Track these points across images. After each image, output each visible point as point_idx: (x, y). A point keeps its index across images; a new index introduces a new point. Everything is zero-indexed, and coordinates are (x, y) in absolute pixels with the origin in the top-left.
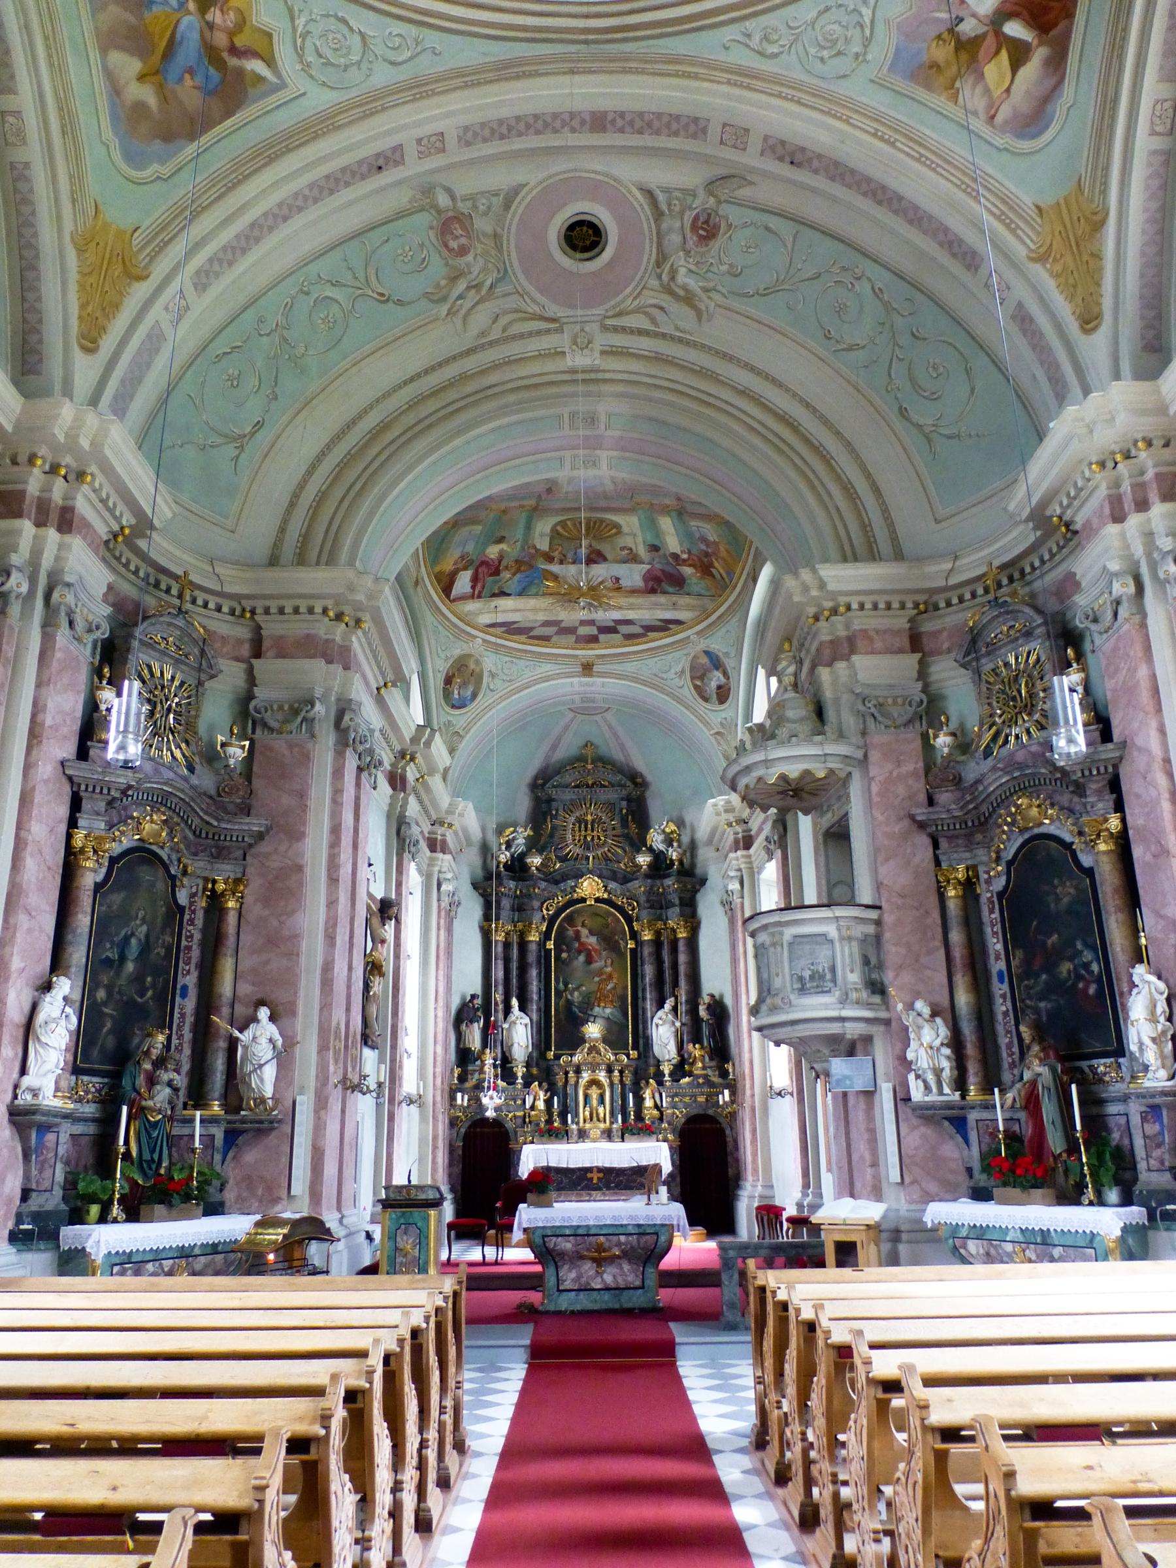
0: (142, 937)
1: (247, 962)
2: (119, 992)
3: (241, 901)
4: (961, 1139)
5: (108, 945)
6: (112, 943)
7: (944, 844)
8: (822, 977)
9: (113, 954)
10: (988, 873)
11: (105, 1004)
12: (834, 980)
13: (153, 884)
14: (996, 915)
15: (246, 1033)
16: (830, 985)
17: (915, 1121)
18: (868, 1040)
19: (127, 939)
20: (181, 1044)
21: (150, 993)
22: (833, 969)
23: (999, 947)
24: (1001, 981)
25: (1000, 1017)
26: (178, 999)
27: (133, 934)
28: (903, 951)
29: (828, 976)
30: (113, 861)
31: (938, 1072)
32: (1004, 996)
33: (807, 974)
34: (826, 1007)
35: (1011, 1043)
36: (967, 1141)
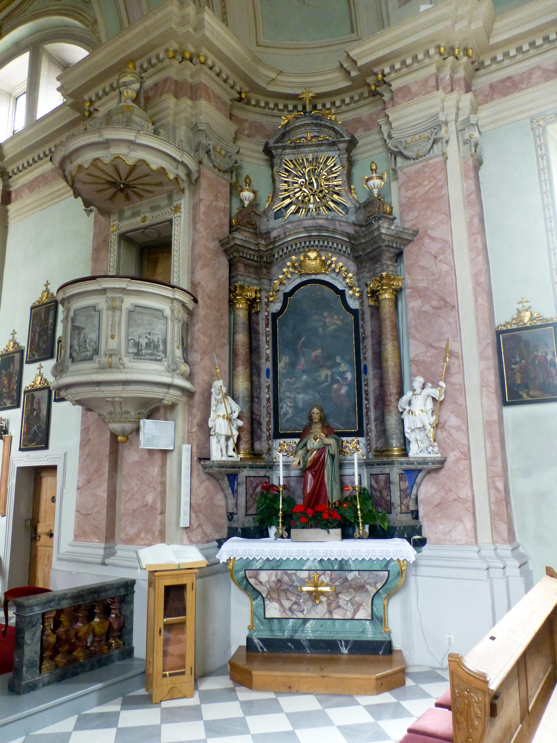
4: (229, 491)
7: (241, 269)
8: (156, 347)
10: (268, 298)
12: (165, 351)
14: (269, 329)
16: (162, 355)
17: (204, 477)
18: (173, 407)
22: (165, 342)
23: (269, 352)
24: (268, 376)
25: (264, 402)
28: (207, 341)
29: (161, 347)
31: (228, 438)
32: (268, 387)
33: (143, 341)
34: (159, 373)
35: (269, 421)
36: (234, 492)
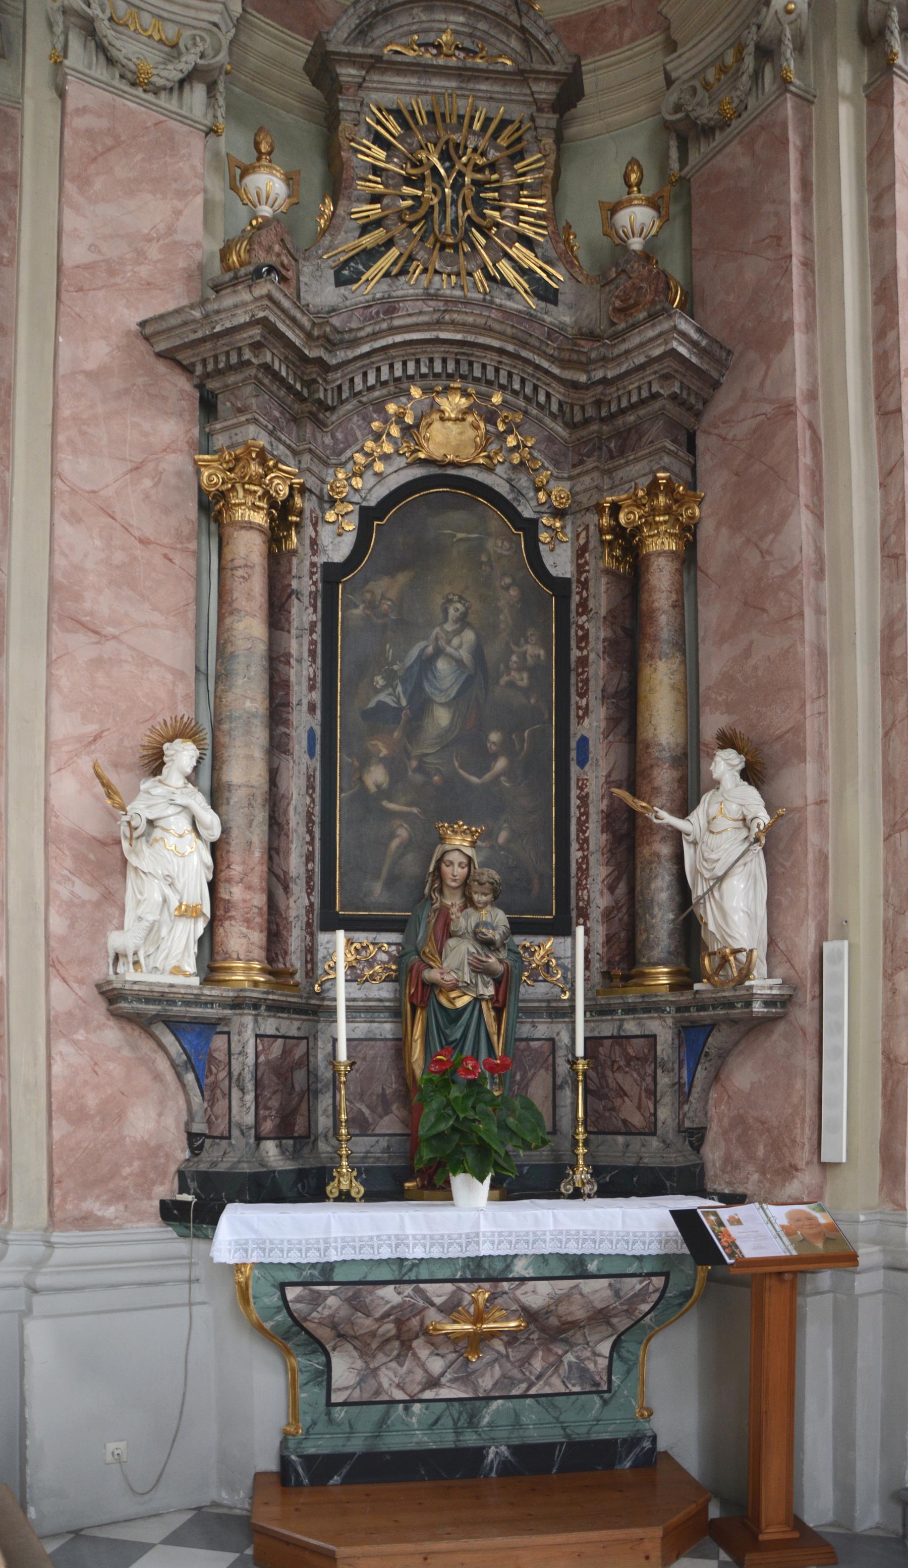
0: (464, 654)
1: (714, 664)
2: (420, 769)
3: (689, 536)
5: (380, 681)
6: (391, 678)
9: (389, 696)
11: (384, 793)
13: (478, 547)
15: (693, 817)
19: (426, 663)
20: (585, 858)
21: (501, 764)
26: (574, 768)
27: (439, 652)
30: (367, 516)
